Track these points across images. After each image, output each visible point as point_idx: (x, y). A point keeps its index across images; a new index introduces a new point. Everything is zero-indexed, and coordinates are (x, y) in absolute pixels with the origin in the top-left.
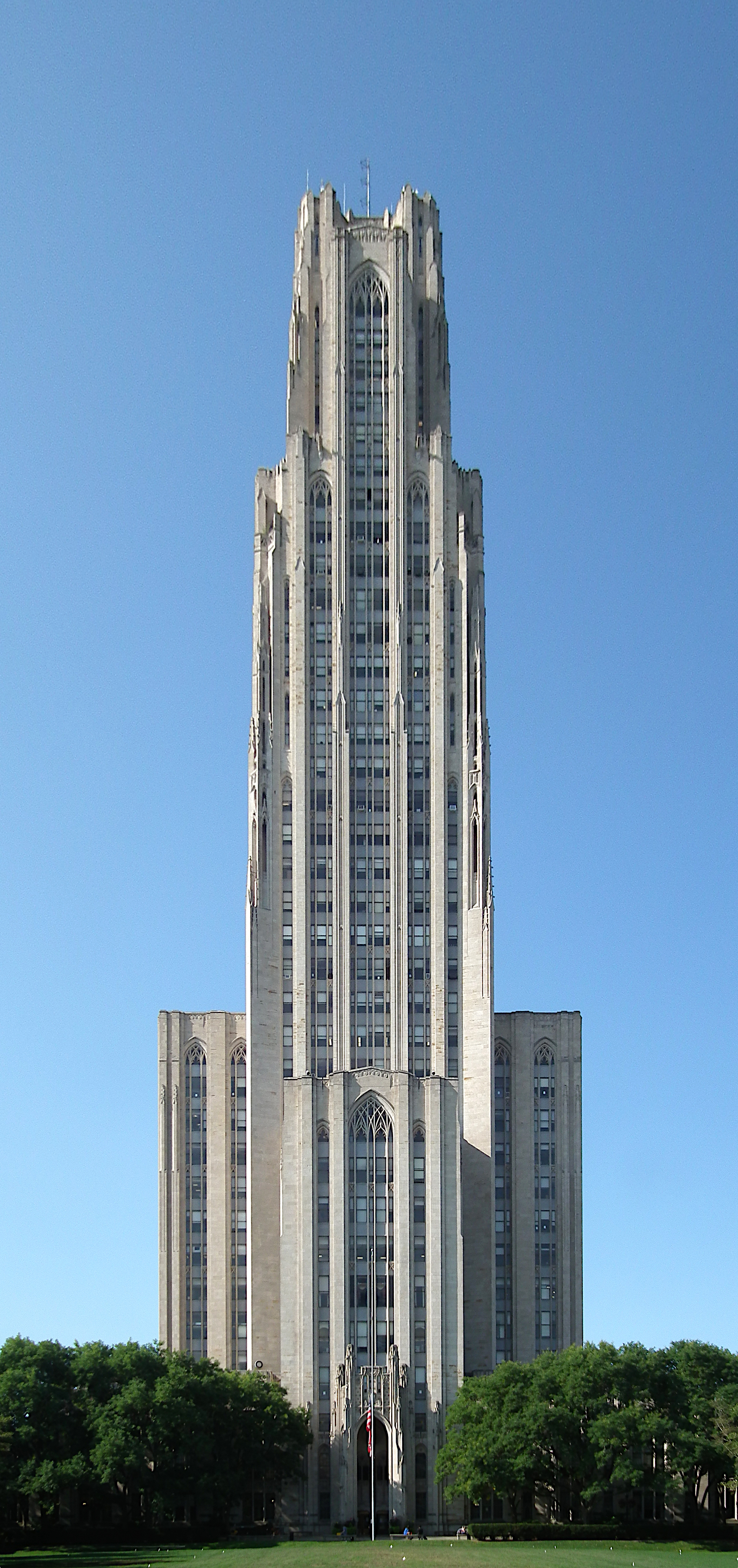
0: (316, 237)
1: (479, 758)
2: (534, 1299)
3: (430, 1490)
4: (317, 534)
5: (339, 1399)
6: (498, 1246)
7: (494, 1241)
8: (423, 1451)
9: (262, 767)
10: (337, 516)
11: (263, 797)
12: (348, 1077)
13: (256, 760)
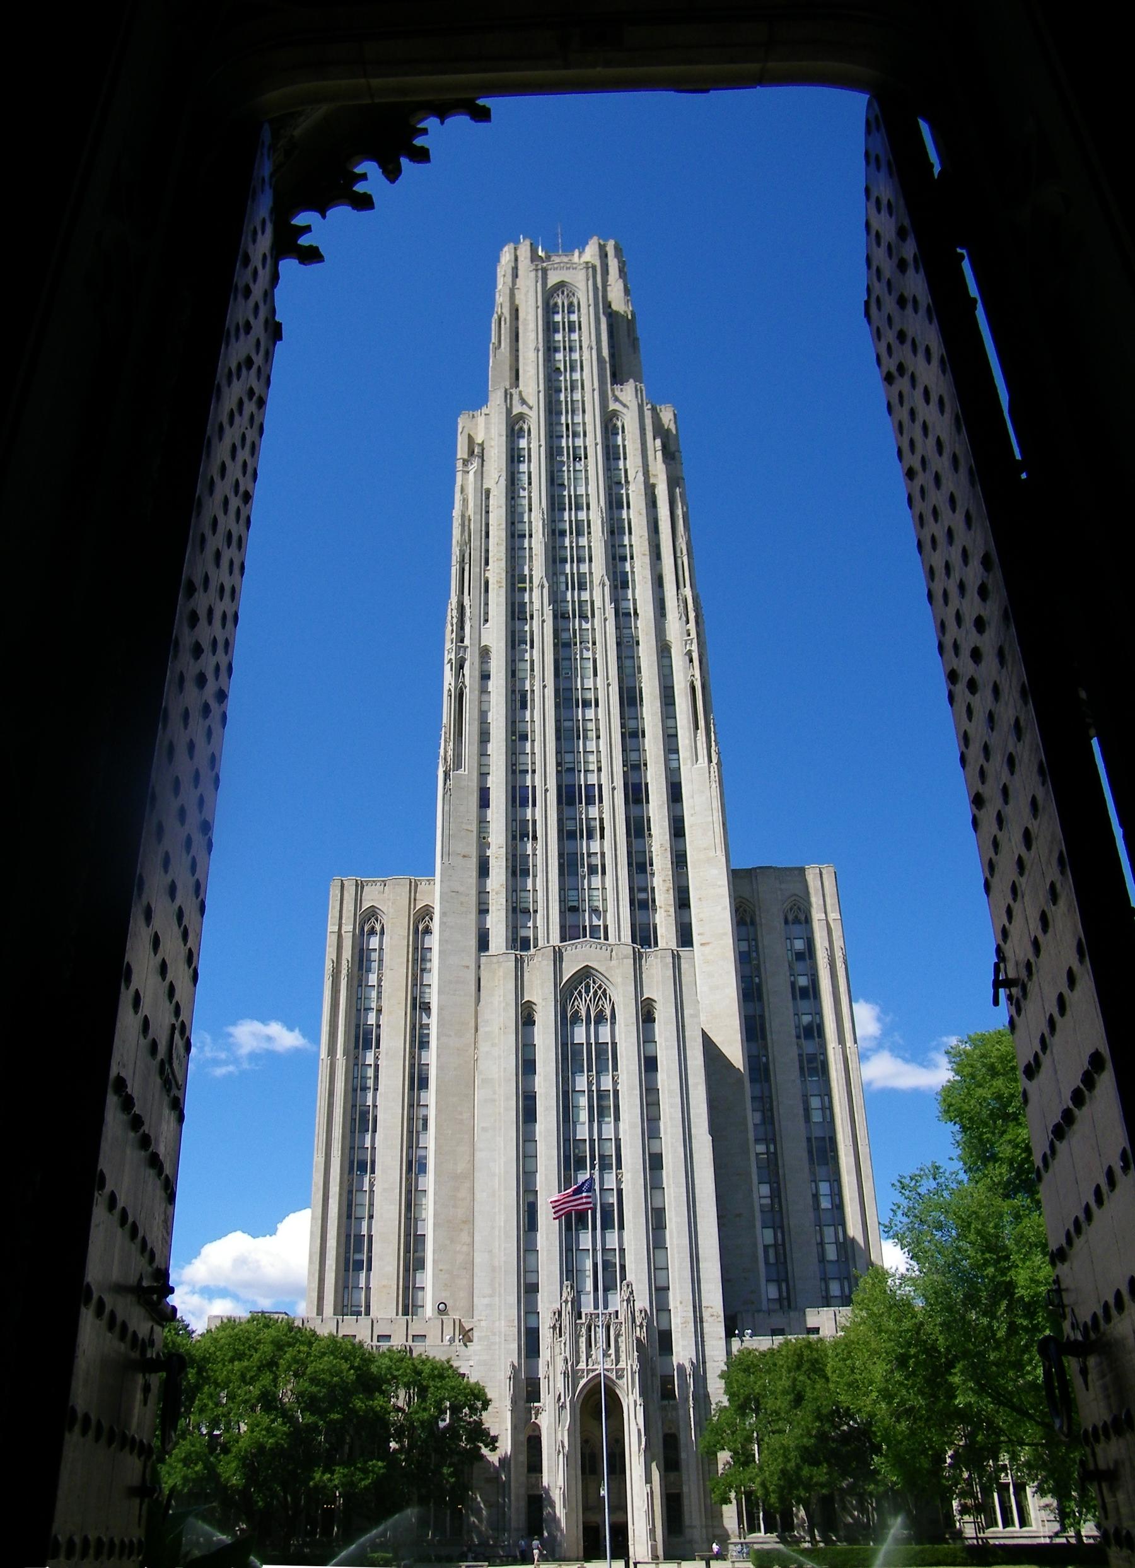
2: (811, 1209)
3: (685, 1489)
5: (553, 1357)
6: (757, 1141)
7: (751, 1136)
8: (673, 1431)
12: (558, 957)
13: (454, 635)
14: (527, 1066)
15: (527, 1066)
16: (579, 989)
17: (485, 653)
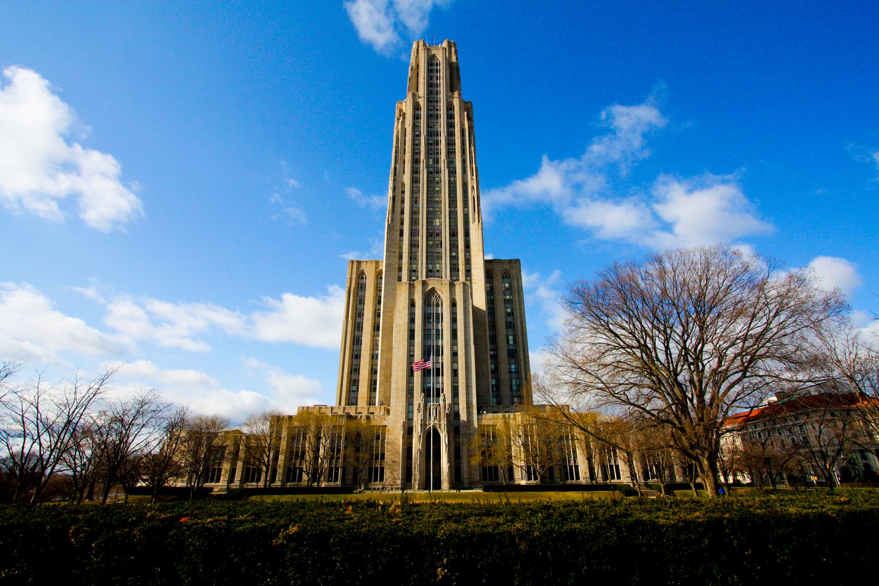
0: (418, 50)
1: (474, 177)
4: (416, 117)
9: (395, 180)
10: (423, 113)
11: (394, 189)
14: (412, 320)
15: (412, 320)
16: (429, 296)
17: (403, 185)
